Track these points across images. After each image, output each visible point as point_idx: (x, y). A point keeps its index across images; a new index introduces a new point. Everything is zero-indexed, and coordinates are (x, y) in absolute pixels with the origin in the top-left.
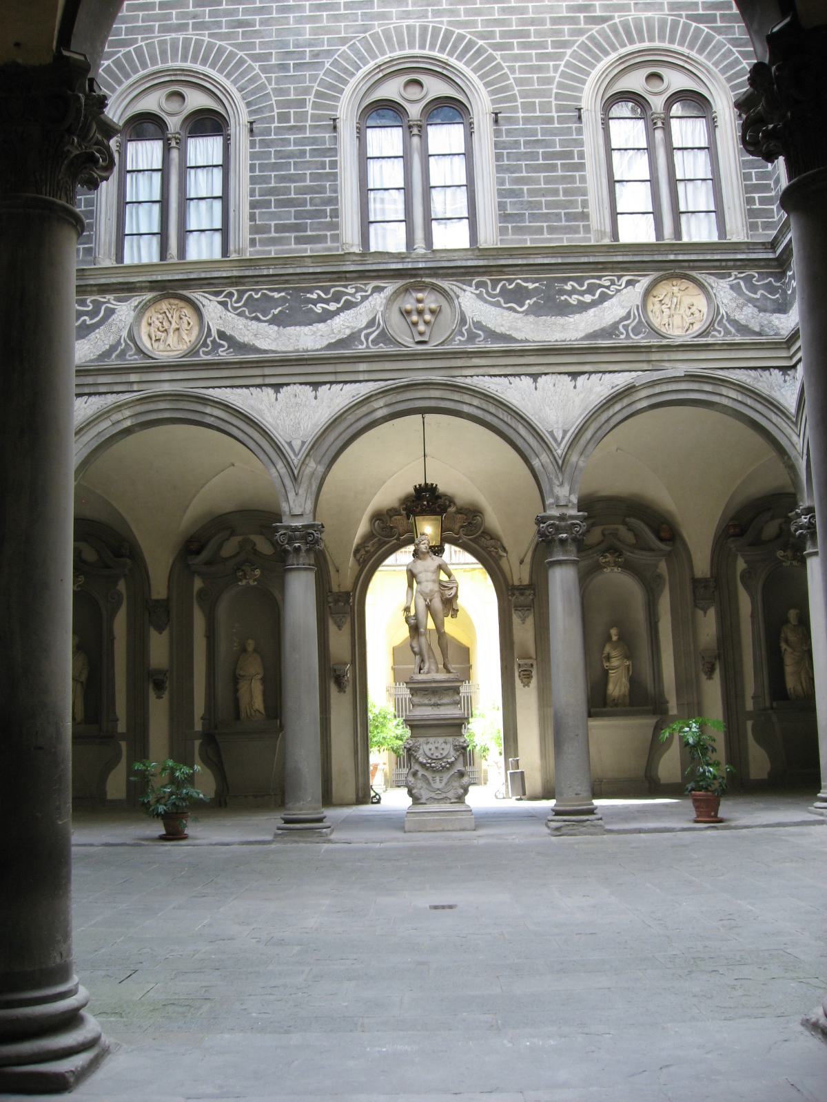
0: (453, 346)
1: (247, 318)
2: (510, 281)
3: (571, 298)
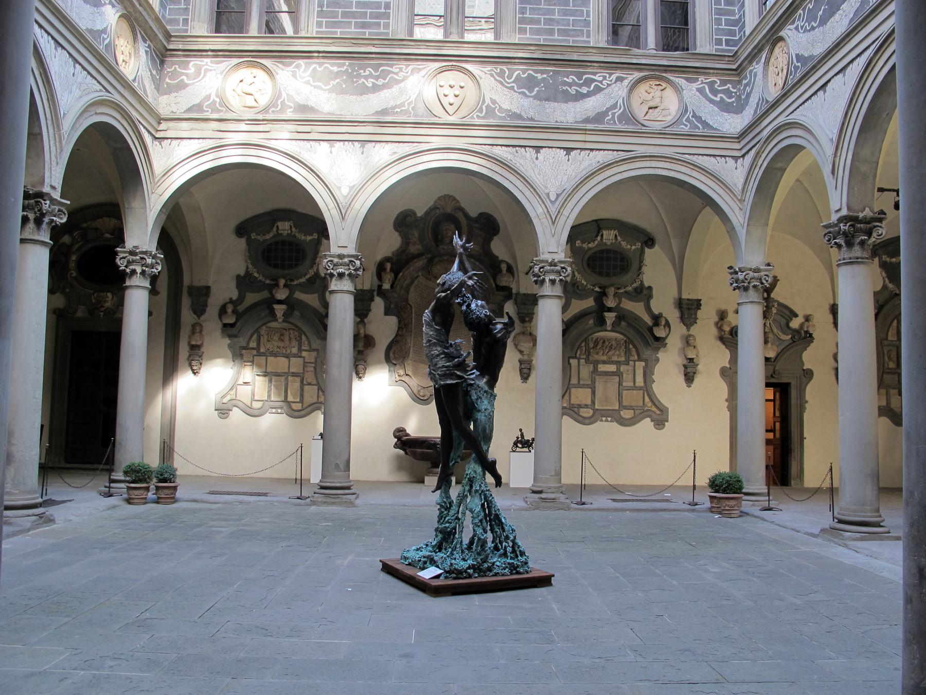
1: (312, 86)
2: (524, 71)
3: (571, 88)
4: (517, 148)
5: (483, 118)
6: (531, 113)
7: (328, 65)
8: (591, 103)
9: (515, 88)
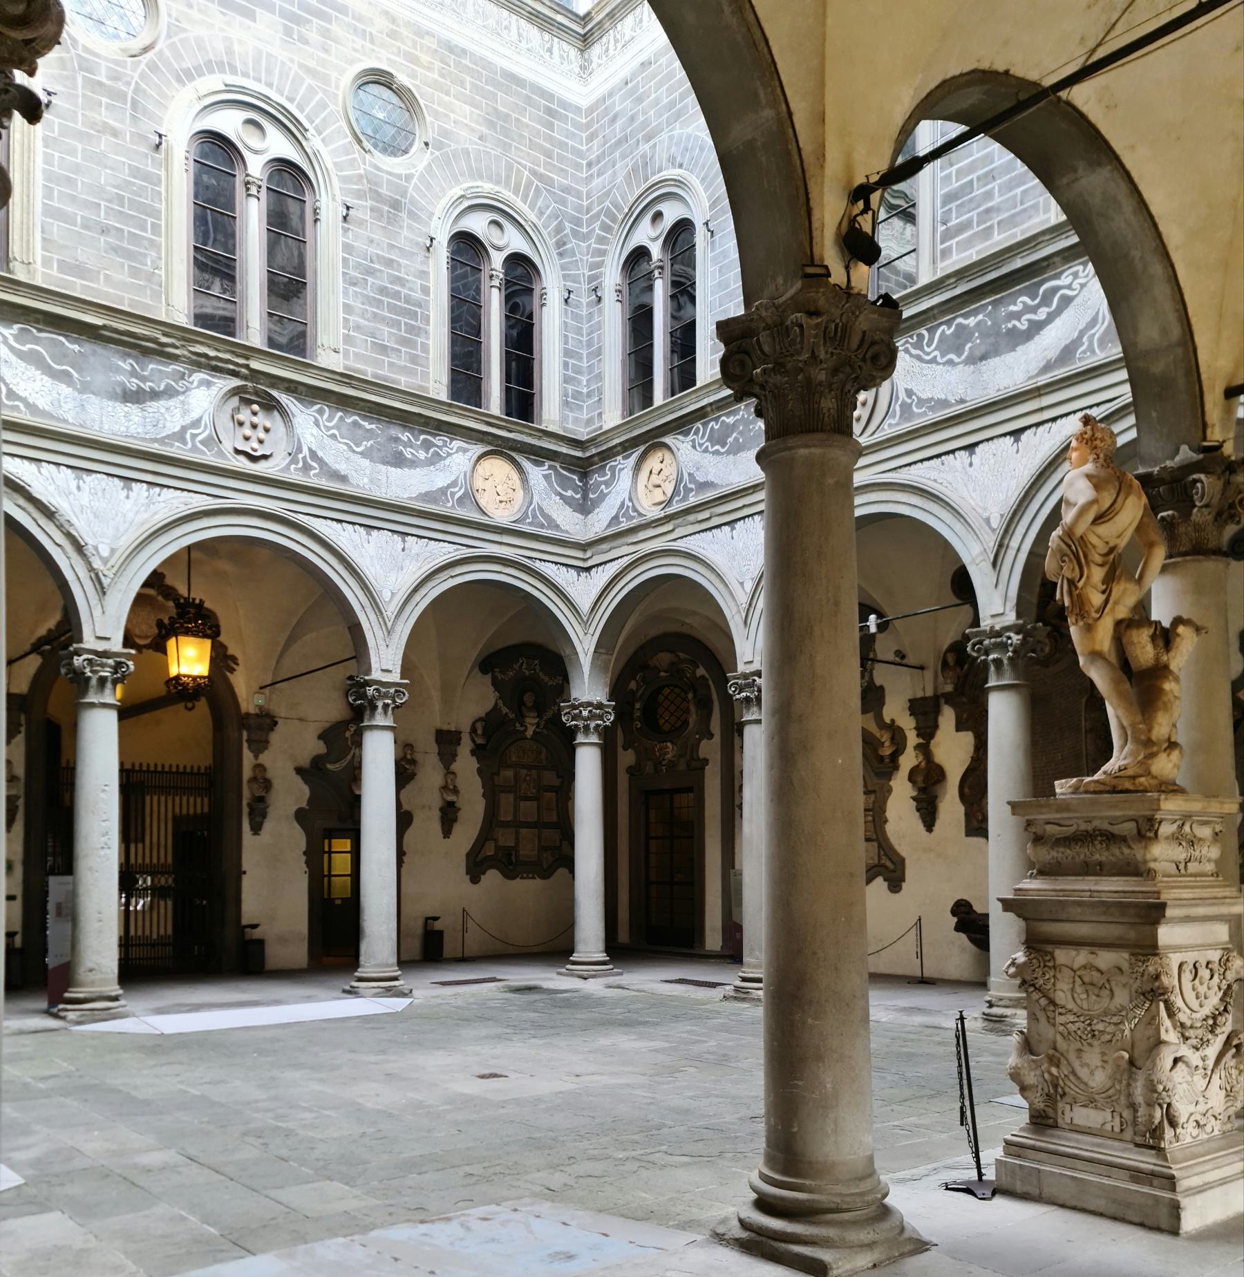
0: (888, 431)
3: (1019, 320)
4: (943, 458)
5: (897, 424)
6: (960, 392)
8: (1053, 333)
9: (939, 359)
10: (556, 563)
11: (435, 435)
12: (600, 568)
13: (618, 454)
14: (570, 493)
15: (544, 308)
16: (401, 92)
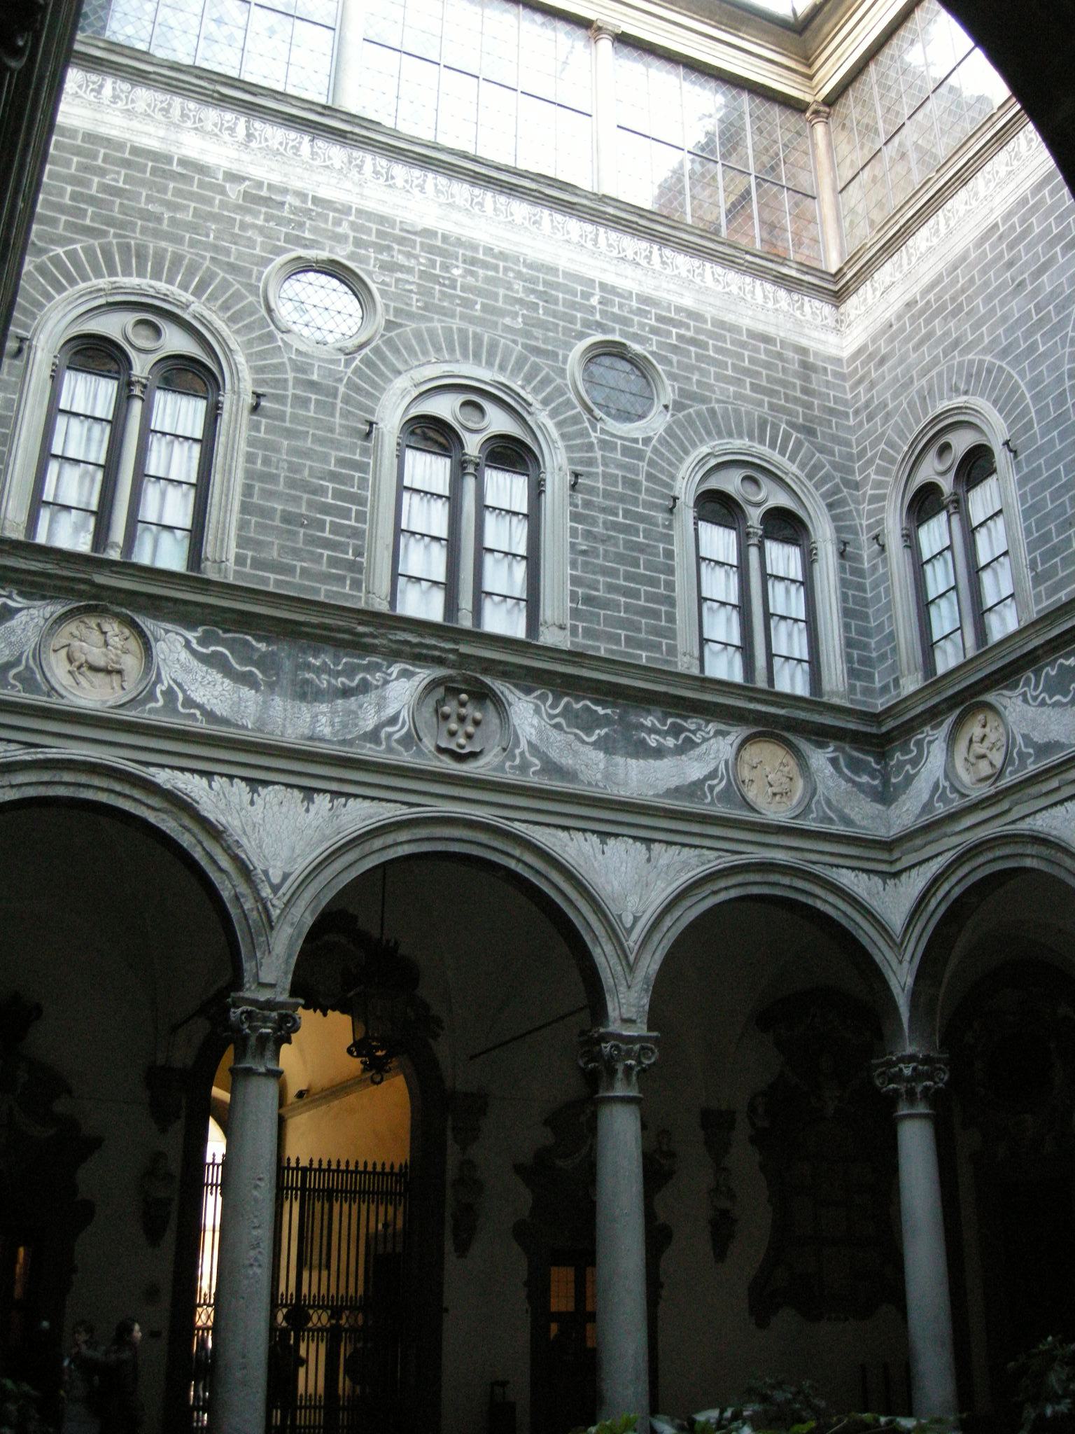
7: (1061, 661)
10: (853, 869)
11: (685, 718)
12: (914, 872)
13: (924, 724)
14: (865, 779)
15: (816, 566)
16: (639, 364)
